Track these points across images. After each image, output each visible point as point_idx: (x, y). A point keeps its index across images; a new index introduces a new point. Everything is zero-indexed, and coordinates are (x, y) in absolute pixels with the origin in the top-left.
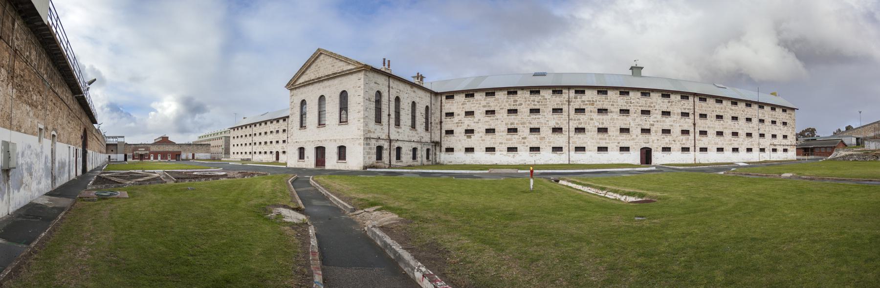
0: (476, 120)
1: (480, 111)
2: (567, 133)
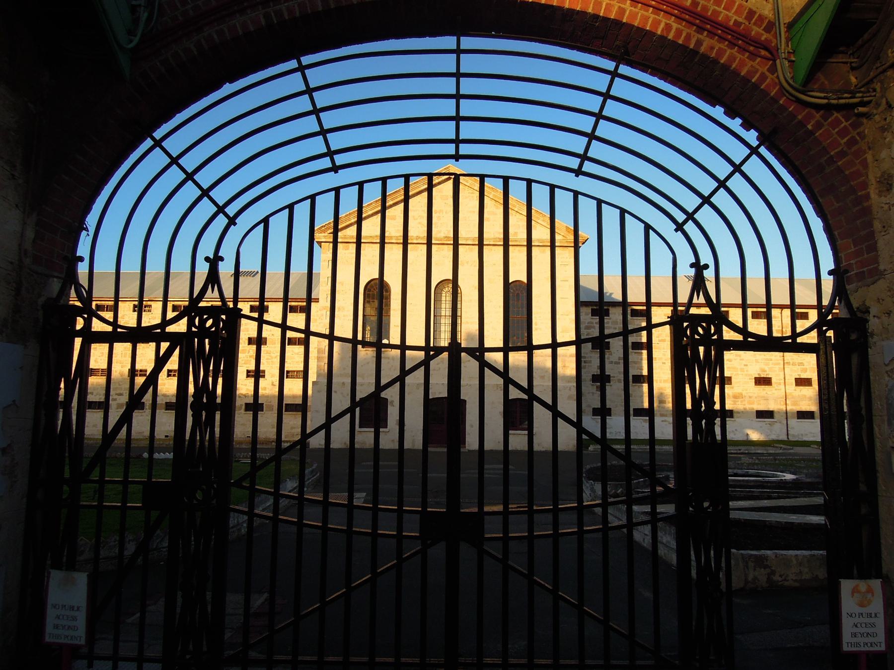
2: (782, 387)
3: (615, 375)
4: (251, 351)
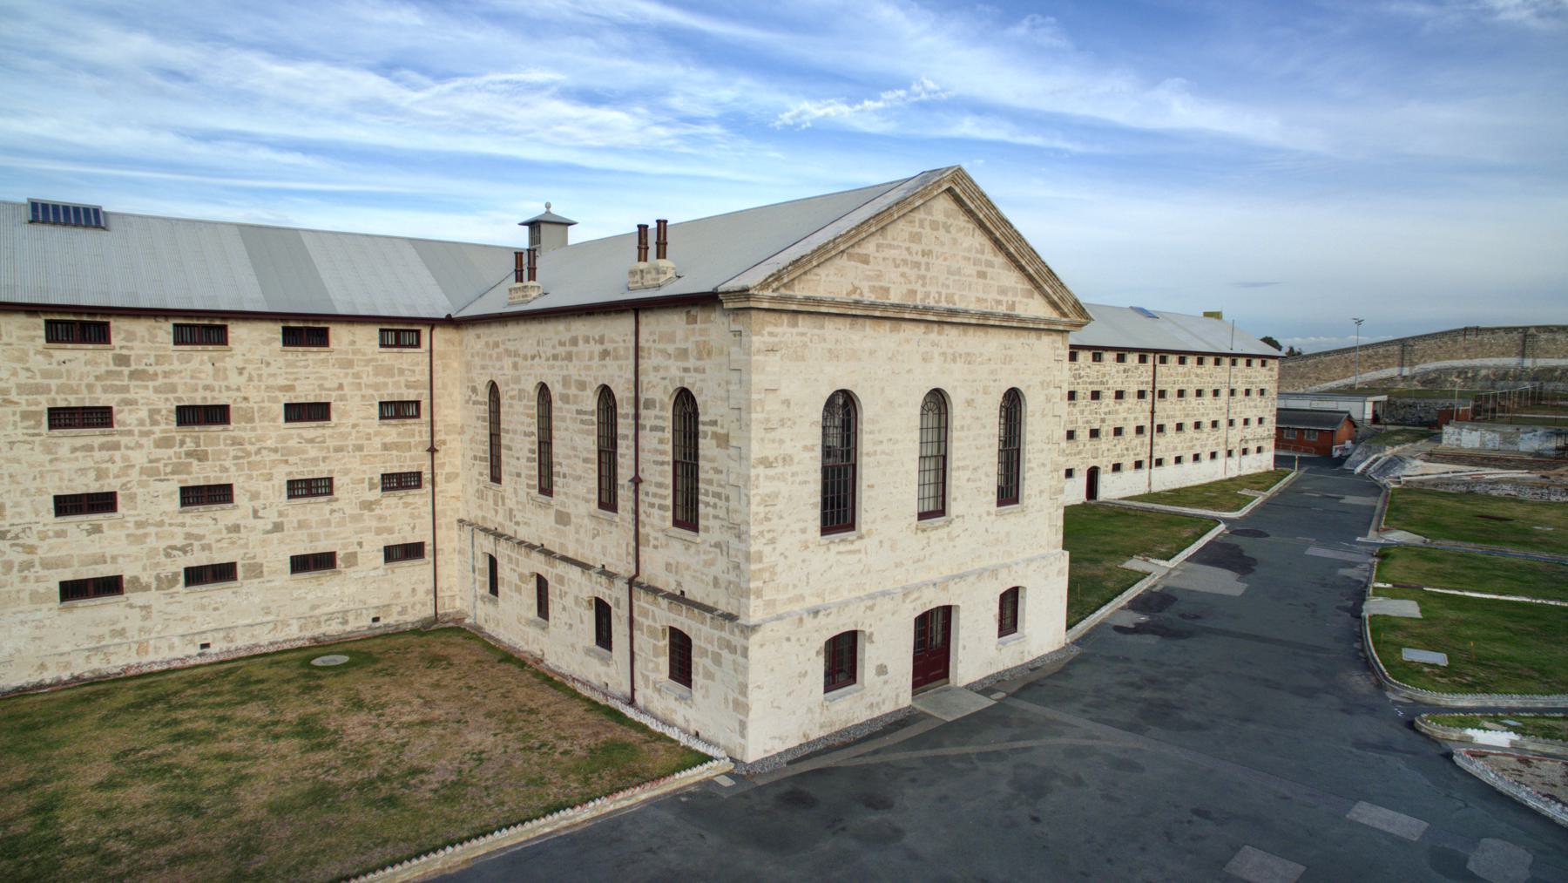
4: (188, 440)
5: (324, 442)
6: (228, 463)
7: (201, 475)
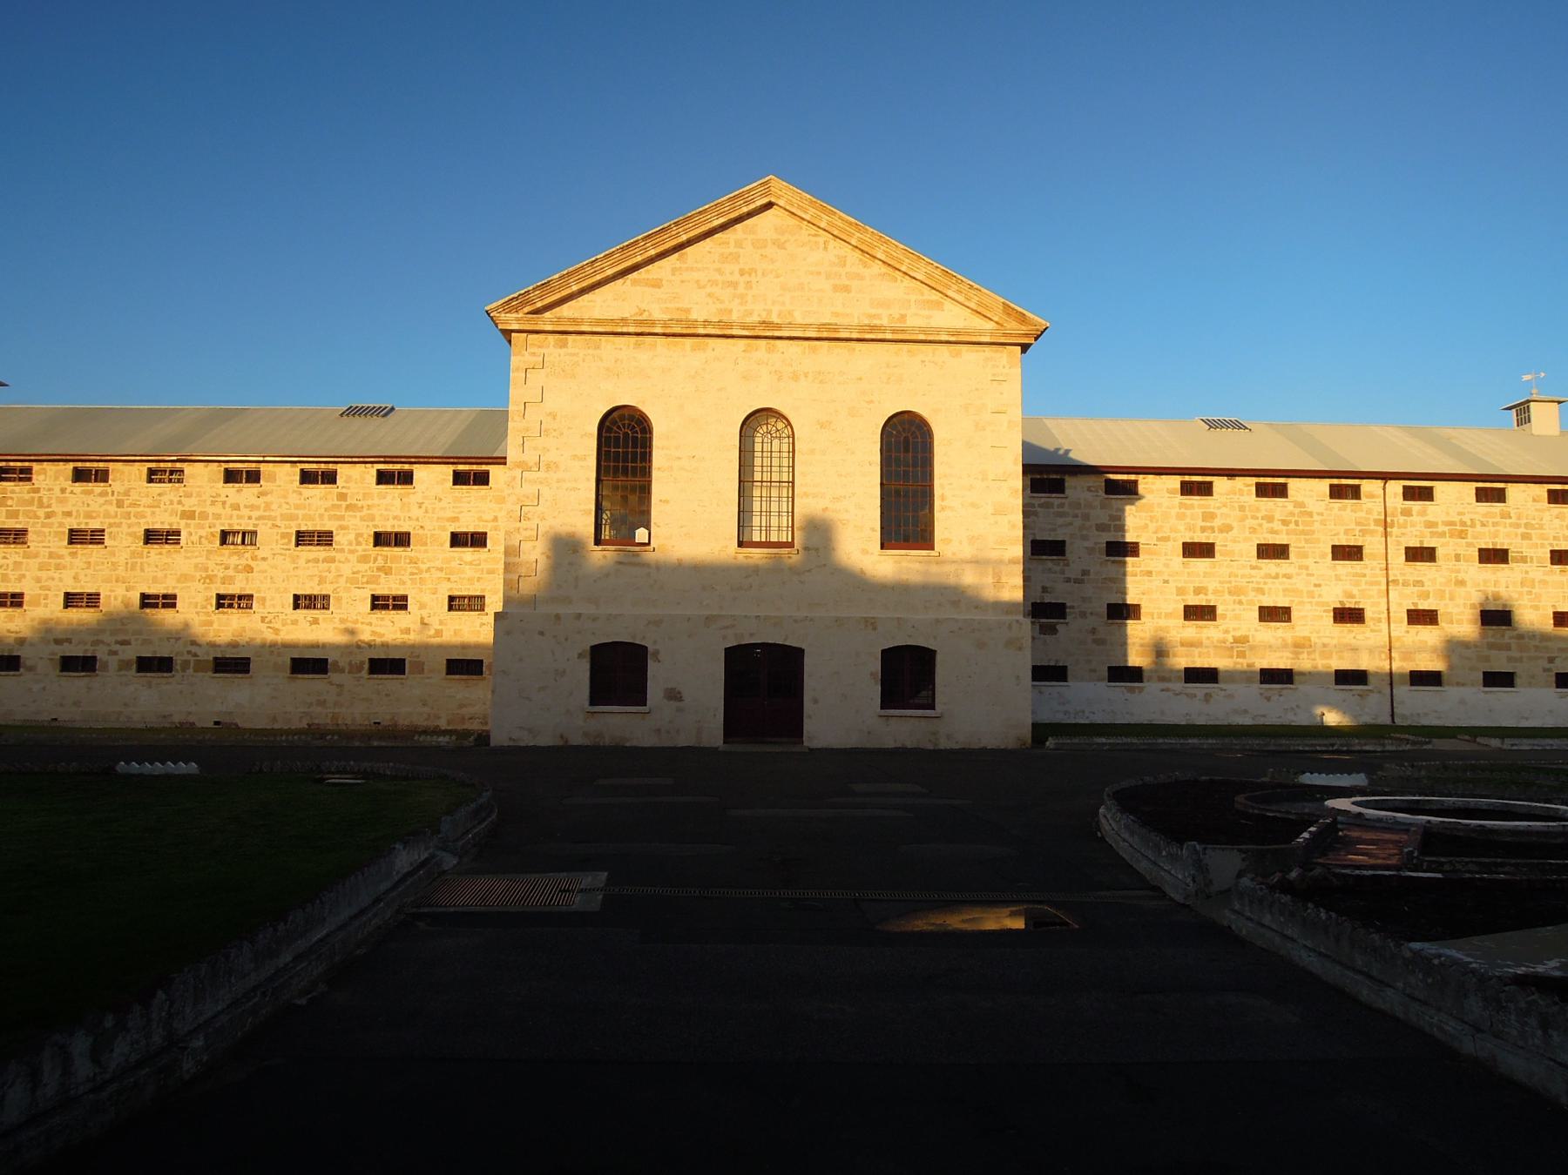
0: (1073, 571)
1: (1086, 544)
2: (1384, 626)
3: (1075, 604)
4: (379, 558)
5: (479, 565)
6: (406, 578)
7: (387, 587)
